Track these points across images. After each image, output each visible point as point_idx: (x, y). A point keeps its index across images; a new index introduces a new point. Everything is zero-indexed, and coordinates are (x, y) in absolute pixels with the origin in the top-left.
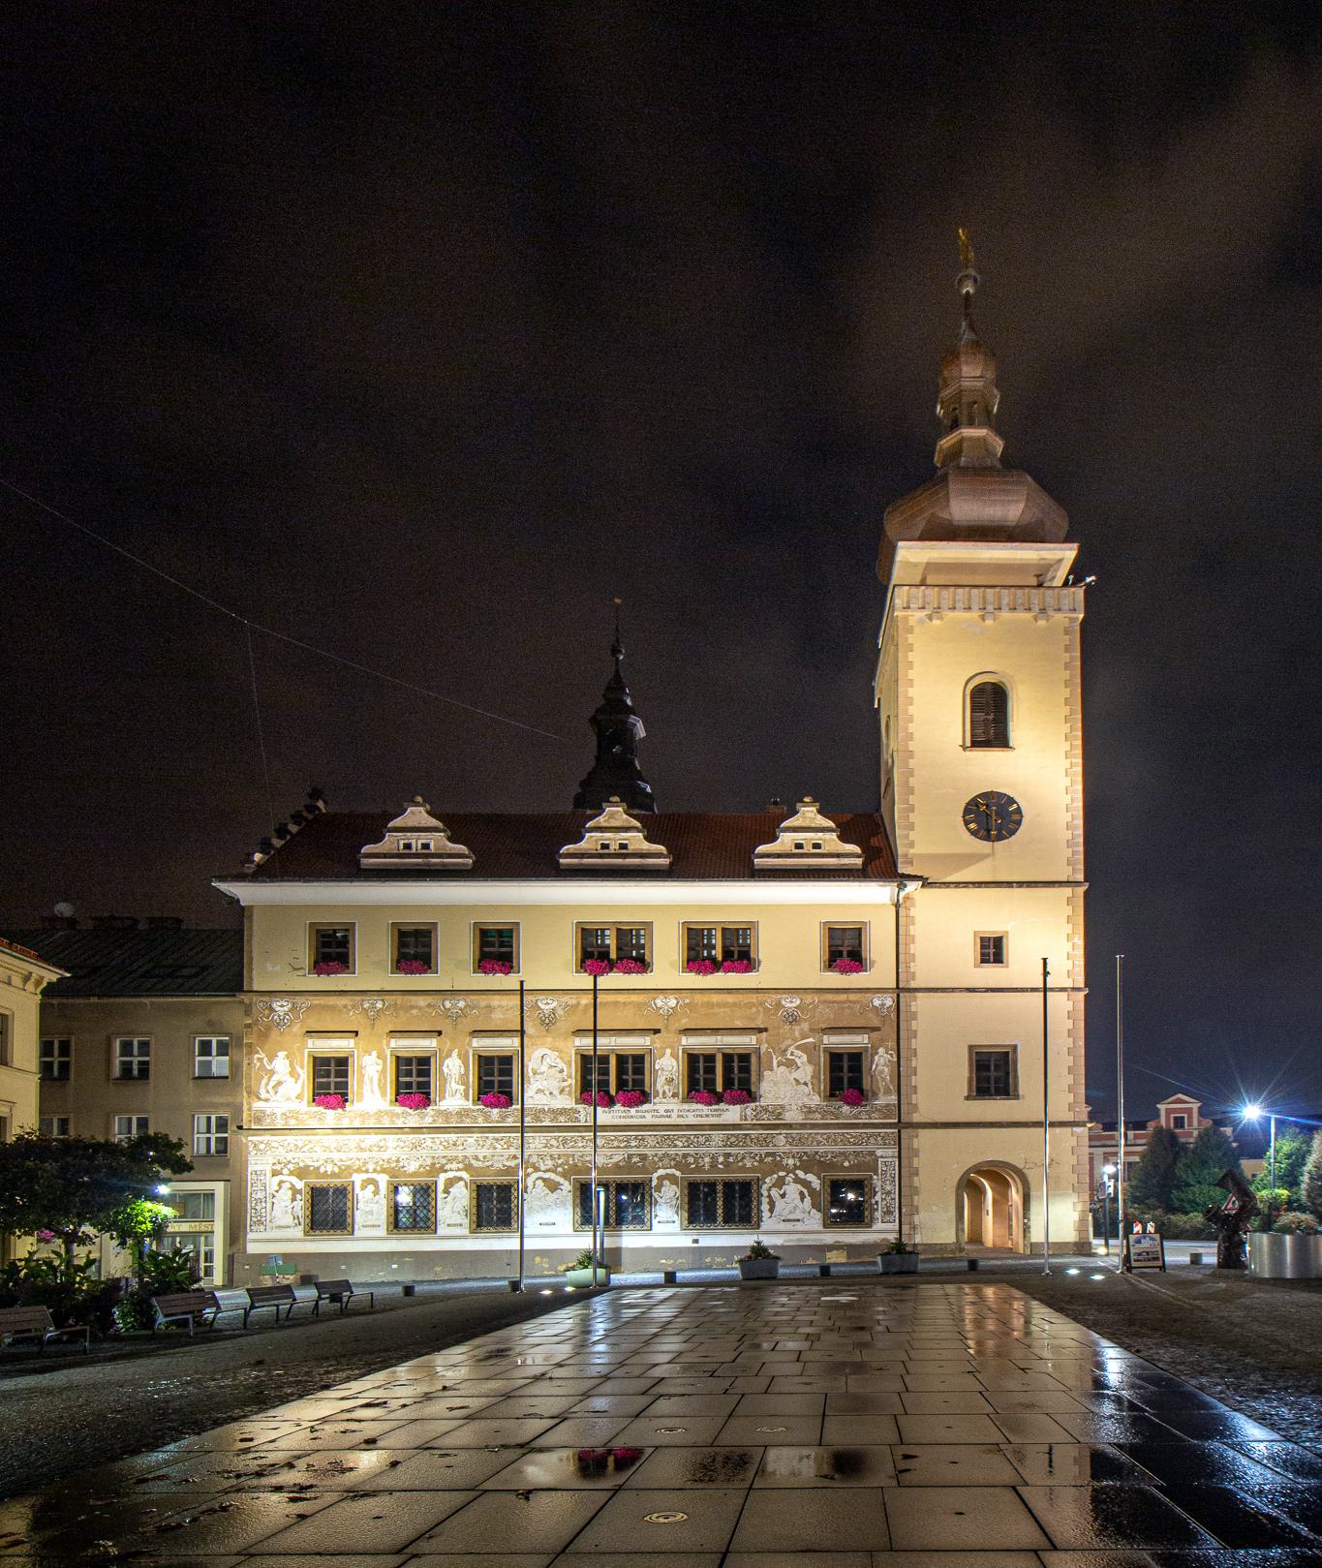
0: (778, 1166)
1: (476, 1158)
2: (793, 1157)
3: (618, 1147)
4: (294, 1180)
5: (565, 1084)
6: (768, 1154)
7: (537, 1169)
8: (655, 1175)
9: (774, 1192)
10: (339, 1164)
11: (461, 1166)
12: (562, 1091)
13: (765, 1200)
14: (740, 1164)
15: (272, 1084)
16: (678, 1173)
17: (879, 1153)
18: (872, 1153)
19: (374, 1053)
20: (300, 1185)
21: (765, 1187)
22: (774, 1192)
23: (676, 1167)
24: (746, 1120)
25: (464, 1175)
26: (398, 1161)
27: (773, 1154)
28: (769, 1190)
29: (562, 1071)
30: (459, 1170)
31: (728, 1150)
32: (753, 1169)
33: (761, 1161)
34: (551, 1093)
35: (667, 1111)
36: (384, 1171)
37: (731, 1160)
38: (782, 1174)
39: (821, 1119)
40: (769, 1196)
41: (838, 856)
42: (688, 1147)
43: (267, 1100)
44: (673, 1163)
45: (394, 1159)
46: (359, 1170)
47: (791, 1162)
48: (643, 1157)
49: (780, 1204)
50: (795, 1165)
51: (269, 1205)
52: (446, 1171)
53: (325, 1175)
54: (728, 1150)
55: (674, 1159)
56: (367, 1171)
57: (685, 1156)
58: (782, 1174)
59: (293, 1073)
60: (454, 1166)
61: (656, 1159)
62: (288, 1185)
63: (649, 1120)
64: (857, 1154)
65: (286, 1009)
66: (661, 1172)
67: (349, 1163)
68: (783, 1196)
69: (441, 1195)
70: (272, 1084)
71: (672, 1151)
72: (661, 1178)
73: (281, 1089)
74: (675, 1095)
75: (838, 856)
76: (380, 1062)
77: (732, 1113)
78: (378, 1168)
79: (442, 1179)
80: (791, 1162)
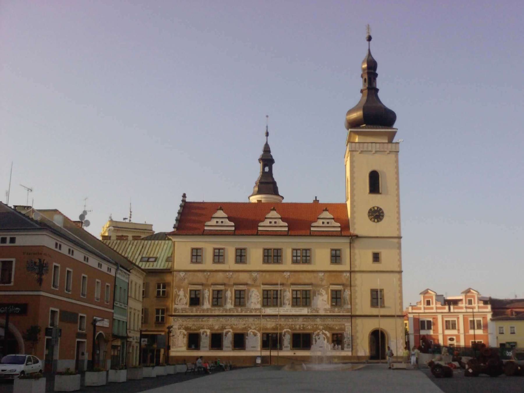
0: (317, 329)
1: (234, 325)
2: (322, 325)
3: (273, 321)
4: (184, 331)
5: (259, 300)
6: (315, 324)
7: (251, 328)
8: (283, 331)
9: (317, 337)
10: (197, 326)
11: (230, 327)
12: (258, 303)
13: (314, 340)
14: (307, 328)
15: (179, 299)
16: (290, 330)
17: (346, 324)
18: (344, 325)
19: (207, 290)
20: (186, 333)
21: (314, 336)
22: (317, 337)
23: (290, 329)
24: (309, 313)
25: (231, 330)
26: (213, 325)
27: (316, 325)
28: (315, 337)
29: (258, 296)
30: (229, 328)
31: (304, 323)
32: (310, 330)
33: (313, 327)
34: (255, 303)
35: (287, 309)
36: (209, 329)
37: (305, 326)
38: (319, 331)
39: (330, 313)
40: (315, 339)
41: (334, 227)
42: (293, 322)
43: (177, 305)
44: (288, 327)
45: (212, 324)
46: (202, 328)
47: (321, 327)
48: (280, 325)
49: (318, 341)
50: (322, 328)
51: (177, 339)
52: (225, 329)
53: (193, 330)
54: (304, 323)
55: (288, 326)
56: (204, 329)
57: (292, 325)
58: (319, 331)
59: (185, 296)
60: (228, 327)
61: (284, 326)
62: (182, 333)
63: (282, 313)
64: (340, 325)
65: (183, 275)
66: (285, 330)
67: (198, 326)
68: (319, 339)
69: (224, 337)
70: (179, 299)
71: (288, 323)
72: (285, 333)
73: (182, 300)
74: (289, 304)
75: (334, 227)
76: (209, 292)
77: (305, 311)
78: (207, 328)
79: (225, 331)
80: (321, 327)
